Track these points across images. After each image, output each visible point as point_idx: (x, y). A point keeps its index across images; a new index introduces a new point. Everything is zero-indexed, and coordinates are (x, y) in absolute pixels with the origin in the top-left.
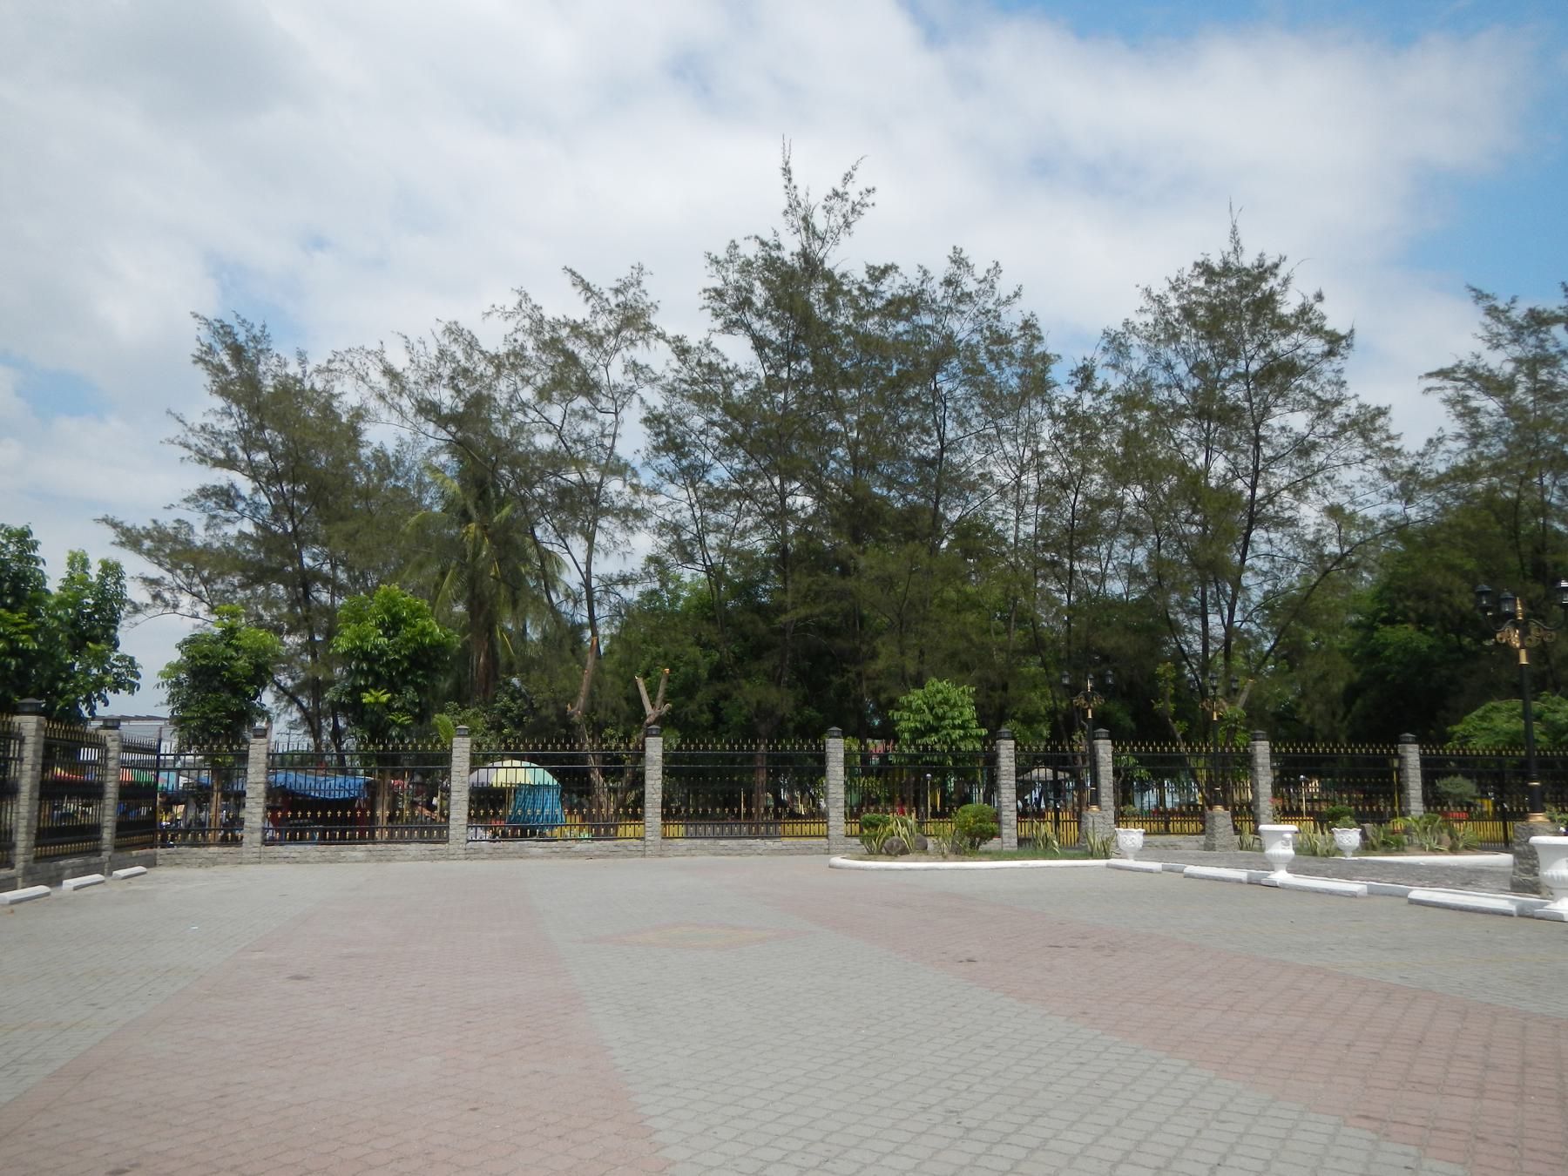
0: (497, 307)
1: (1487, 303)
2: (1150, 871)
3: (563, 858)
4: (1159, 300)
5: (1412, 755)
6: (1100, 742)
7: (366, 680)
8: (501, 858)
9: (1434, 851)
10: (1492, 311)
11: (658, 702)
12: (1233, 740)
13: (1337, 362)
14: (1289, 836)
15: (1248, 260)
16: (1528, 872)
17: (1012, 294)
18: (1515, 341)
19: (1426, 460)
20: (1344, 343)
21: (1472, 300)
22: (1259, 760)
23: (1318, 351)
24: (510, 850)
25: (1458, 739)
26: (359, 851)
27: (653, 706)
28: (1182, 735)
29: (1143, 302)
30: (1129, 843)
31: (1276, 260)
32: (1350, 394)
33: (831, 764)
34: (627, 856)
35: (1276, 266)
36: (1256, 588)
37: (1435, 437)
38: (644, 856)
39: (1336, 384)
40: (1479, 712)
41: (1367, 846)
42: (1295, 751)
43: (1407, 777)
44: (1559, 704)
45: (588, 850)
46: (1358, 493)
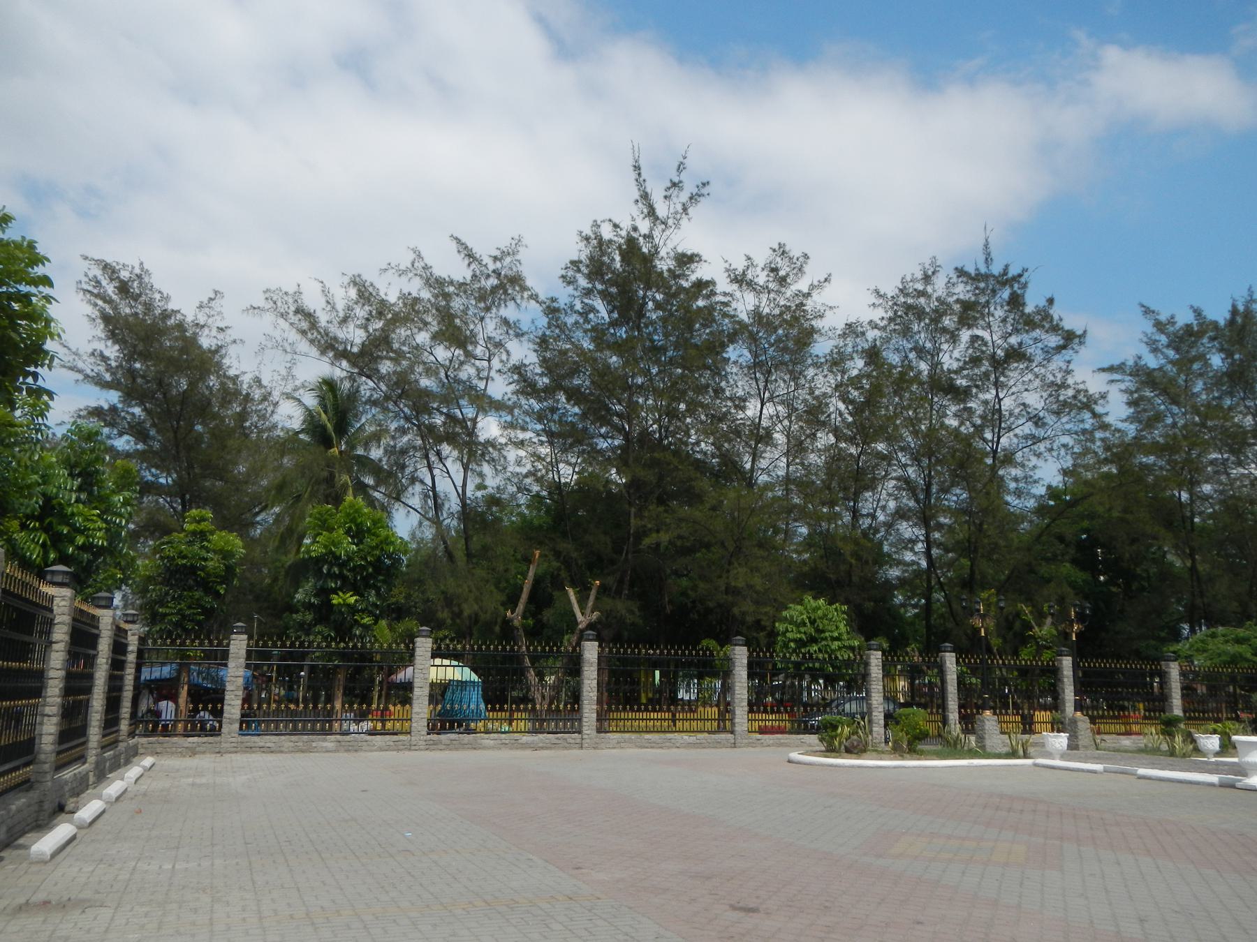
0: (393, 265)
2: (1094, 772)
3: (511, 749)
6: (947, 654)
7: (336, 584)
8: (457, 749)
11: (588, 611)
13: (1067, 354)
17: (822, 280)
20: (1077, 340)
22: (1065, 673)
23: (1053, 344)
24: (466, 742)
26: (329, 742)
27: (583, 614)
31: (1019, 271)
33: (737, 669)
34: (566, 748)
35: (1020, 276)
38: (582, 747)
42: (1100, 665)
43: (1170, 689)
45: (533, 742)
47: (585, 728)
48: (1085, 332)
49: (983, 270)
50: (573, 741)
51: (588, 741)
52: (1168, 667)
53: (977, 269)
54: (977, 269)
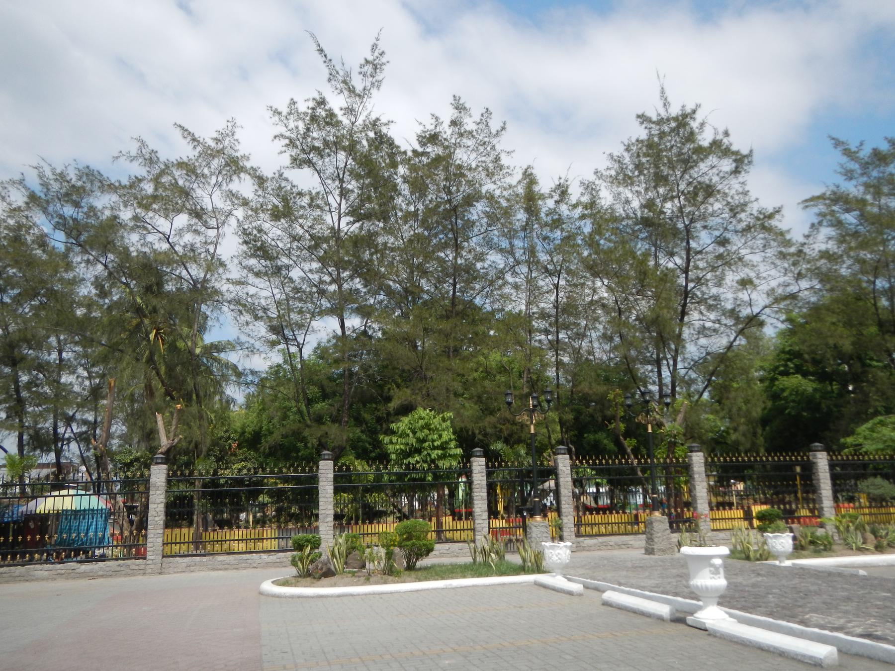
1: (840, 148)
3: (67, 579)
4: (619, 161)
5: (822, 461)
9: (861, 550)
10: (848, 153)
12: (673, 453)
13: (742, 177)
14: (718, 562)
15: (675, 111)
18: (863, 174)
19: (811, 240)
22: (696, 469)
24: (17, 574)
28: (632, 450)
29: (609, 164)
30: (555, 558)
31: (694, 107)
35: (694, 112)
36: (692, 350)
38: (144, 574)
40: (869, 424)
41: (799, 548)
43: (819, 480)
46: (762, 270)
47: (148, 554)
49: (664, 114)
50: (137, 567)
51: (152, 566)
53: (659, 115)
54: (659, 115)
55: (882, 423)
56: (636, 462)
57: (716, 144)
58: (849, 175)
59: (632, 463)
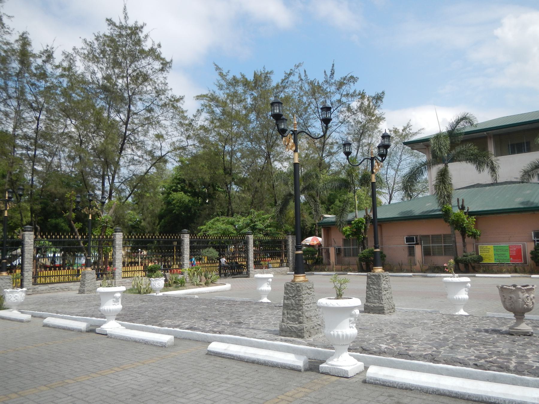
1: (218, 71)
5: (186, 239)
9: (199, 285)
10: (221, 74)
12: (105, 232)
13: (165, 74)
14: (118, 295)
15: (131, 23)
16: (294, 320)
21: (214, 69)
22: (117, 242)
25: (203, 231)
28: (78, 230)
30: (13, 299)
32: (169, 88)
35: (142, 27)
37: (200, 109)
39: (164, 84)
40: (212, 221)
41: (168, 285)
44: (240, 218)
46: (169, 131)
48: (172, 61)
49: (124, 23)
52: (183, 237)
54: (121, 23)
55: (218, 220)
56: (80, 237)
57: (152, 50)
58: (221, 87)
59: (77, 238)
